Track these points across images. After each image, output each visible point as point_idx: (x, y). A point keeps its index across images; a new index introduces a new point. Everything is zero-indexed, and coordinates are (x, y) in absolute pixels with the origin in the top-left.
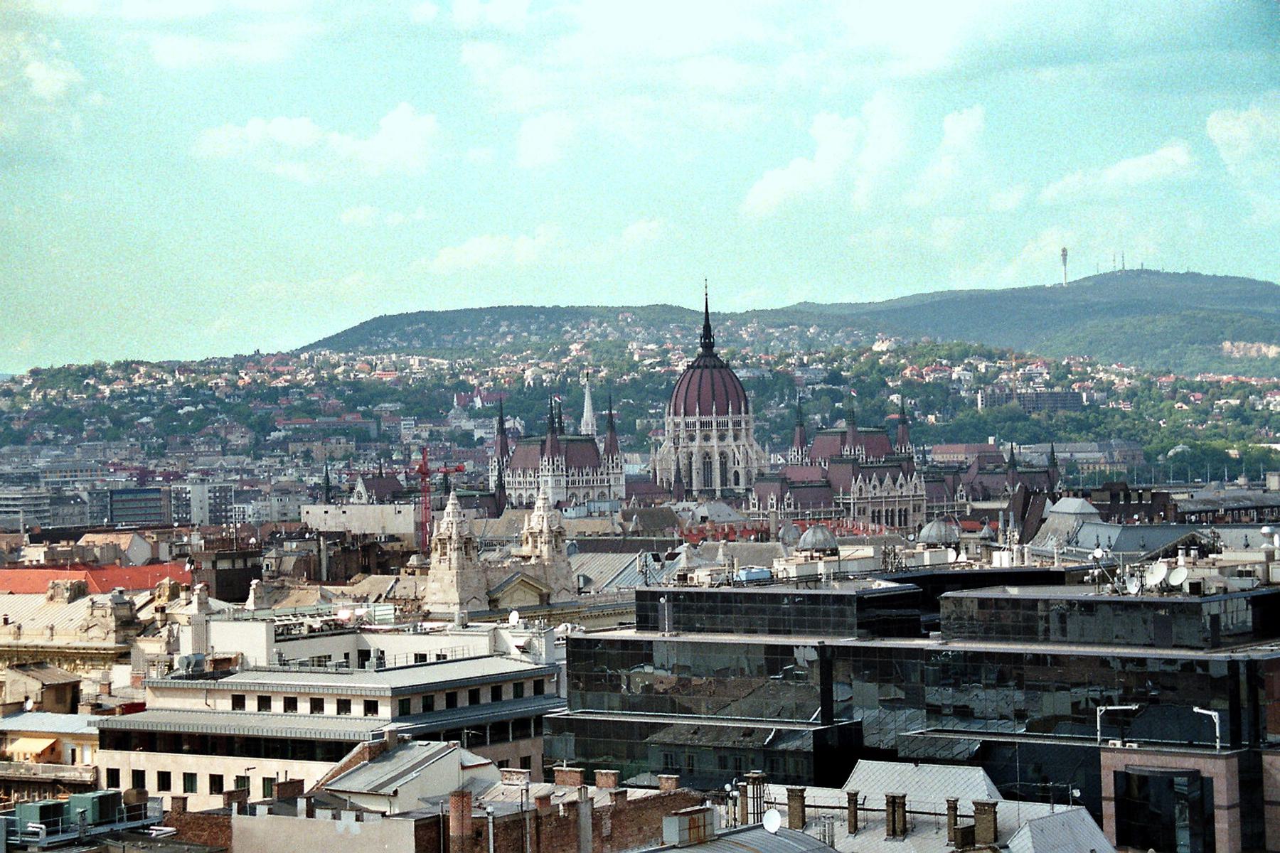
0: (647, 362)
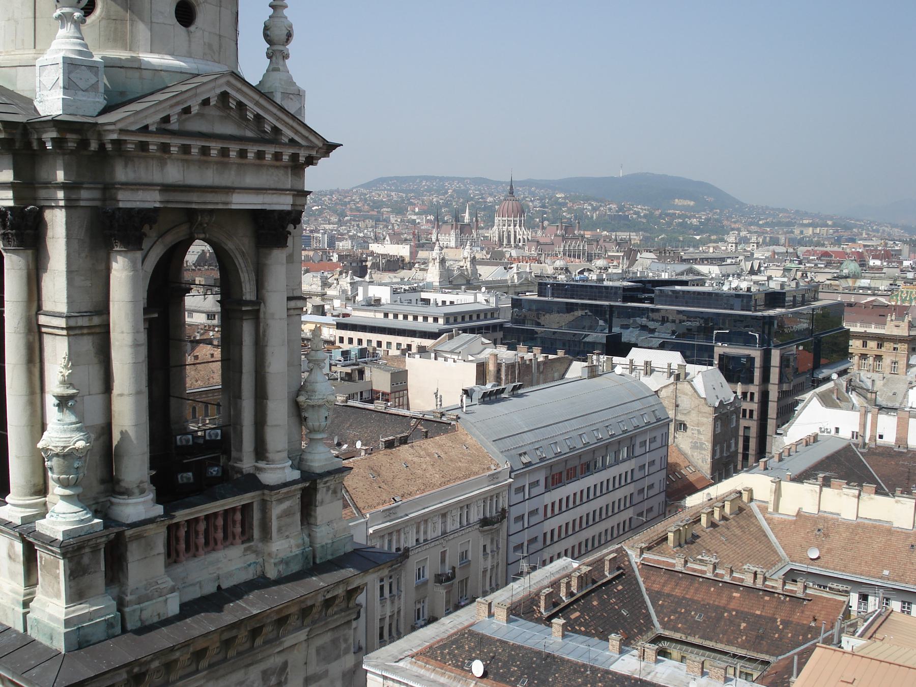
0: (477, 197)
